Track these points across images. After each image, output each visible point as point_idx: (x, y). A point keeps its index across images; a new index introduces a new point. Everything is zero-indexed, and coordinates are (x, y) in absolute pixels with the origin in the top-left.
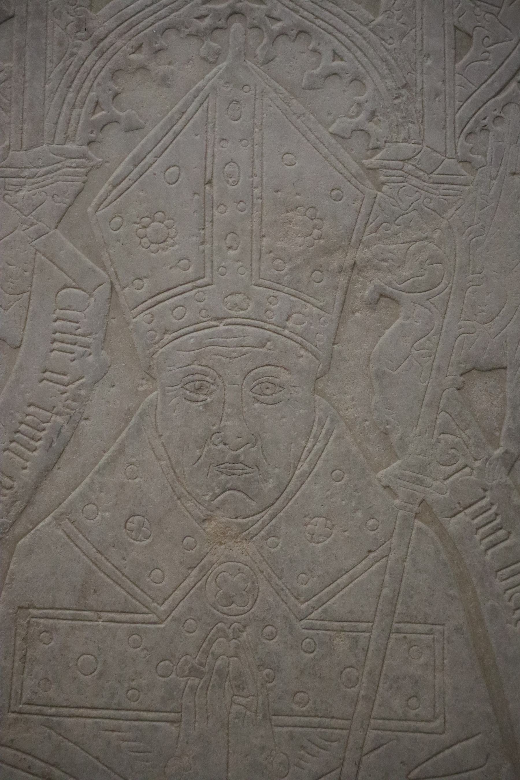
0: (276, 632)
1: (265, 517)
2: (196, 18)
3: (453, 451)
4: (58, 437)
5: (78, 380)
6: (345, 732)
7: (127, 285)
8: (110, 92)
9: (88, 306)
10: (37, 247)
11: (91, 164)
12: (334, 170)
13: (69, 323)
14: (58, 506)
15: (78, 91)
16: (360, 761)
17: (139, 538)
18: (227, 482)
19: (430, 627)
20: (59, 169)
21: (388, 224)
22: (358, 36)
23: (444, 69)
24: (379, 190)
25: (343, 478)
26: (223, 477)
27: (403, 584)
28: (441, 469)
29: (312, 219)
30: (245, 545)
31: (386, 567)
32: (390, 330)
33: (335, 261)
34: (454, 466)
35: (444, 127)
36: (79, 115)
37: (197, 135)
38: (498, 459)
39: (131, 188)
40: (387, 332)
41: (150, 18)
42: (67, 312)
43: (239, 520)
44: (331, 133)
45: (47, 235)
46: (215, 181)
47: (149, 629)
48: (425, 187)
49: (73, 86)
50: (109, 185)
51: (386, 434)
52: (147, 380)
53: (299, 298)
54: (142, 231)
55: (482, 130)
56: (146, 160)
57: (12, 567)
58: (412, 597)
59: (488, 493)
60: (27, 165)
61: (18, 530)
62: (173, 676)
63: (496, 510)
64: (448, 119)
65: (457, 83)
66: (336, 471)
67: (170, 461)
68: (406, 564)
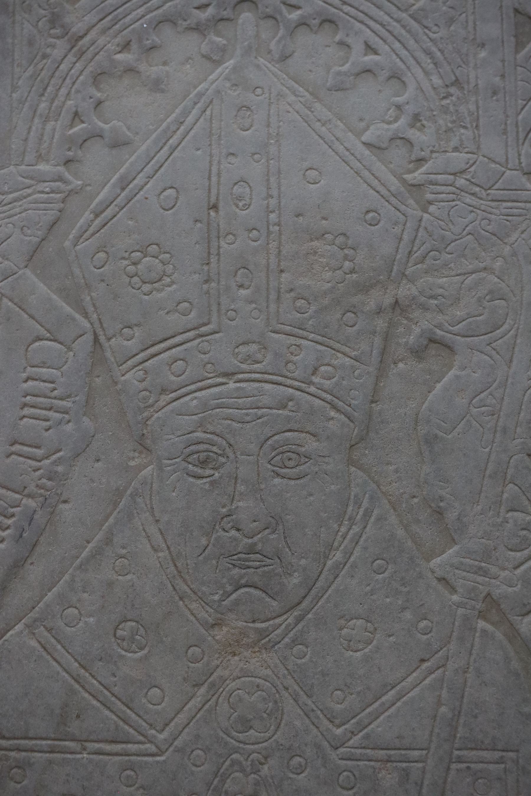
0: (306, 764)
1: (289, 621)
2: (196, 8)
3: (525, 532)
4: (30, 524)
5: (54, 454)
7: (114, 336)
8: (92, 100)
9: (66, 362)
11: (69, 187)
12: (369, 188)
13: (42, 384)
14: (31, 611)
15: (53, 101)
17: (132, 649)
18: (242, 577)
19: (501, 754)
20: (29, 195)
21: (437, 253)
22: (395, 24)
23: (503, 61)
24: (425, 210)
25: (386, 569)
26: (236, 571)
27: (465, 700)
28: (509, 555)
29: (342, 249)
30: (265, 655)
31: (443, 679)
32: (442, 383)
36: (54, 129)
37: (198, 149)
39: (118, 216)
40: (439, 386)
41: (139, 11)
44: (364, 143)
45: (15, 276)
46: (221, 205)
47: (146, 763)
48: (482, 206)
49: (46, 95)
50: (91, 213)
51: (439, 513)
52: (141, 453)
53: (328, 347)
54: (131, 269)
56: (135, 182)
58: (476, 717)
64: (508, 122)
65: (519, 77)
66: (378, 561)
67: (170, 552)
68: (468, 675)
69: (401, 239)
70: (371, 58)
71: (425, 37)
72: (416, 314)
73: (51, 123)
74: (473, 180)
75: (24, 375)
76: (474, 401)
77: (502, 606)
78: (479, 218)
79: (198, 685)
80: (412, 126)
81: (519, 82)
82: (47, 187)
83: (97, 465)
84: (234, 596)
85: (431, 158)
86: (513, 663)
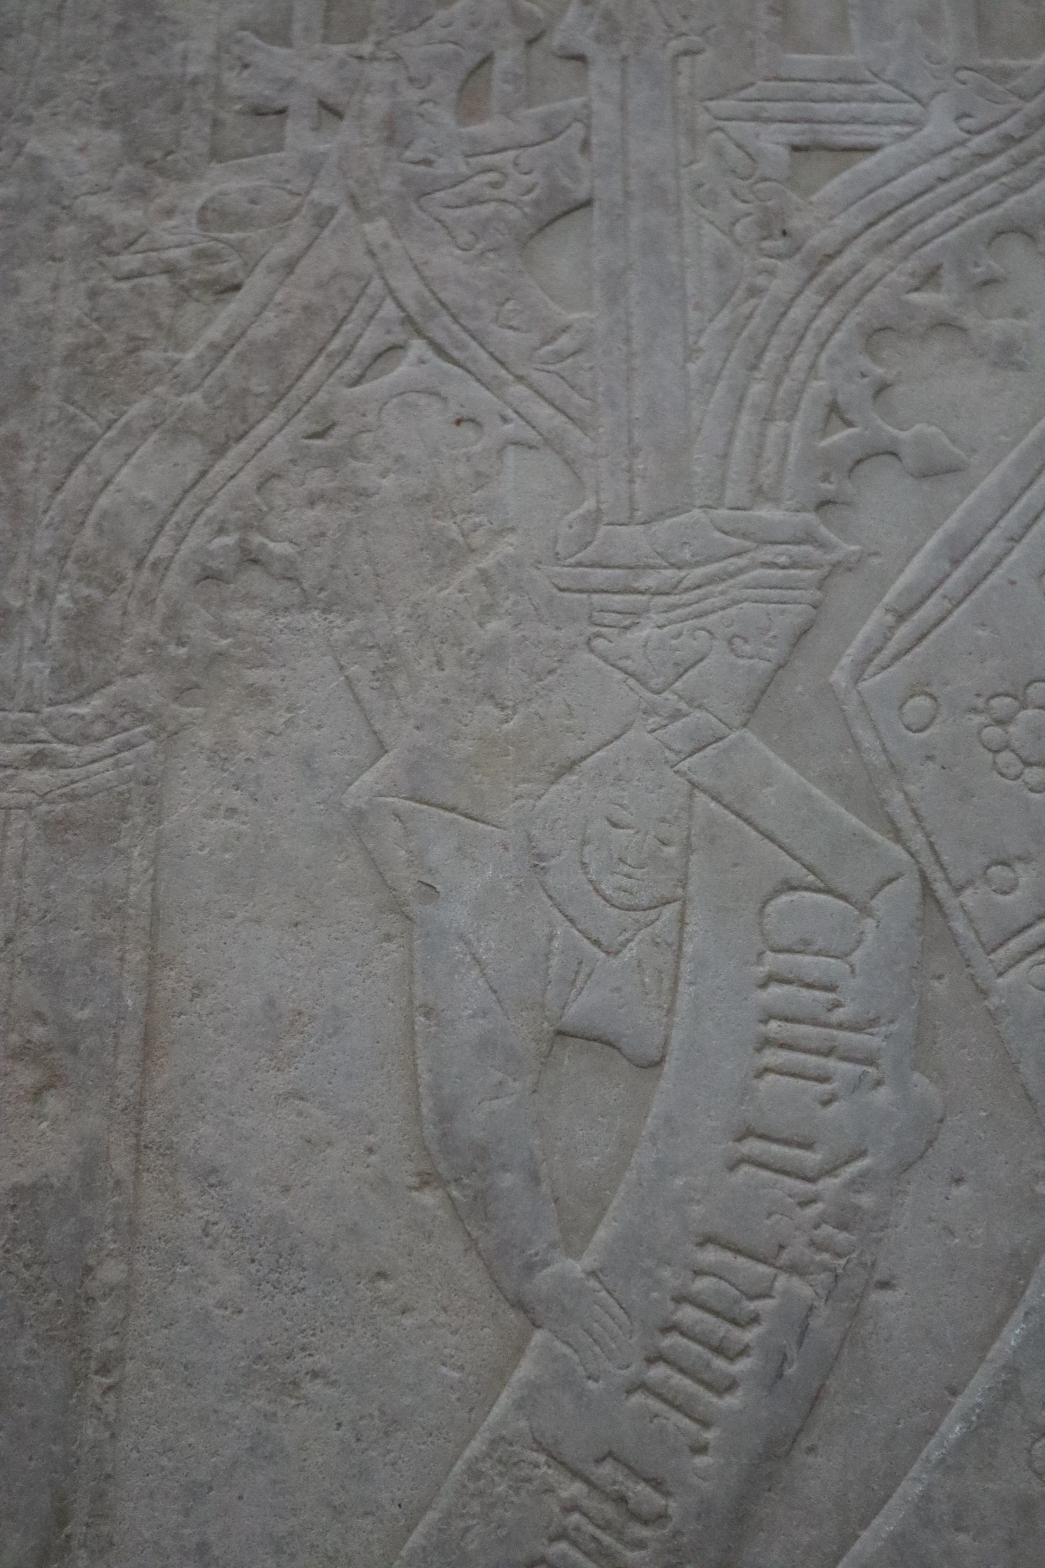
4: (800, 1343)
5: (847, 1163)
7: (970, 883)
8: (866, 380)
9: (859, 942)
10: (695, 778)
11: (834, 557)
13: (805, 992)
15: (778, 381)
20: (741, 571)
36: (787, 437)
39: (951, 620)
41: (951, 210)
42: (799, 957)
45: (720, 744)
49: (763, 366)
54: (993, 733)
56: (984, 547)
60: (651, 561)
73: (778, 423)
75: (763, 970)
82: (782, 554)
83: (956, 1191)
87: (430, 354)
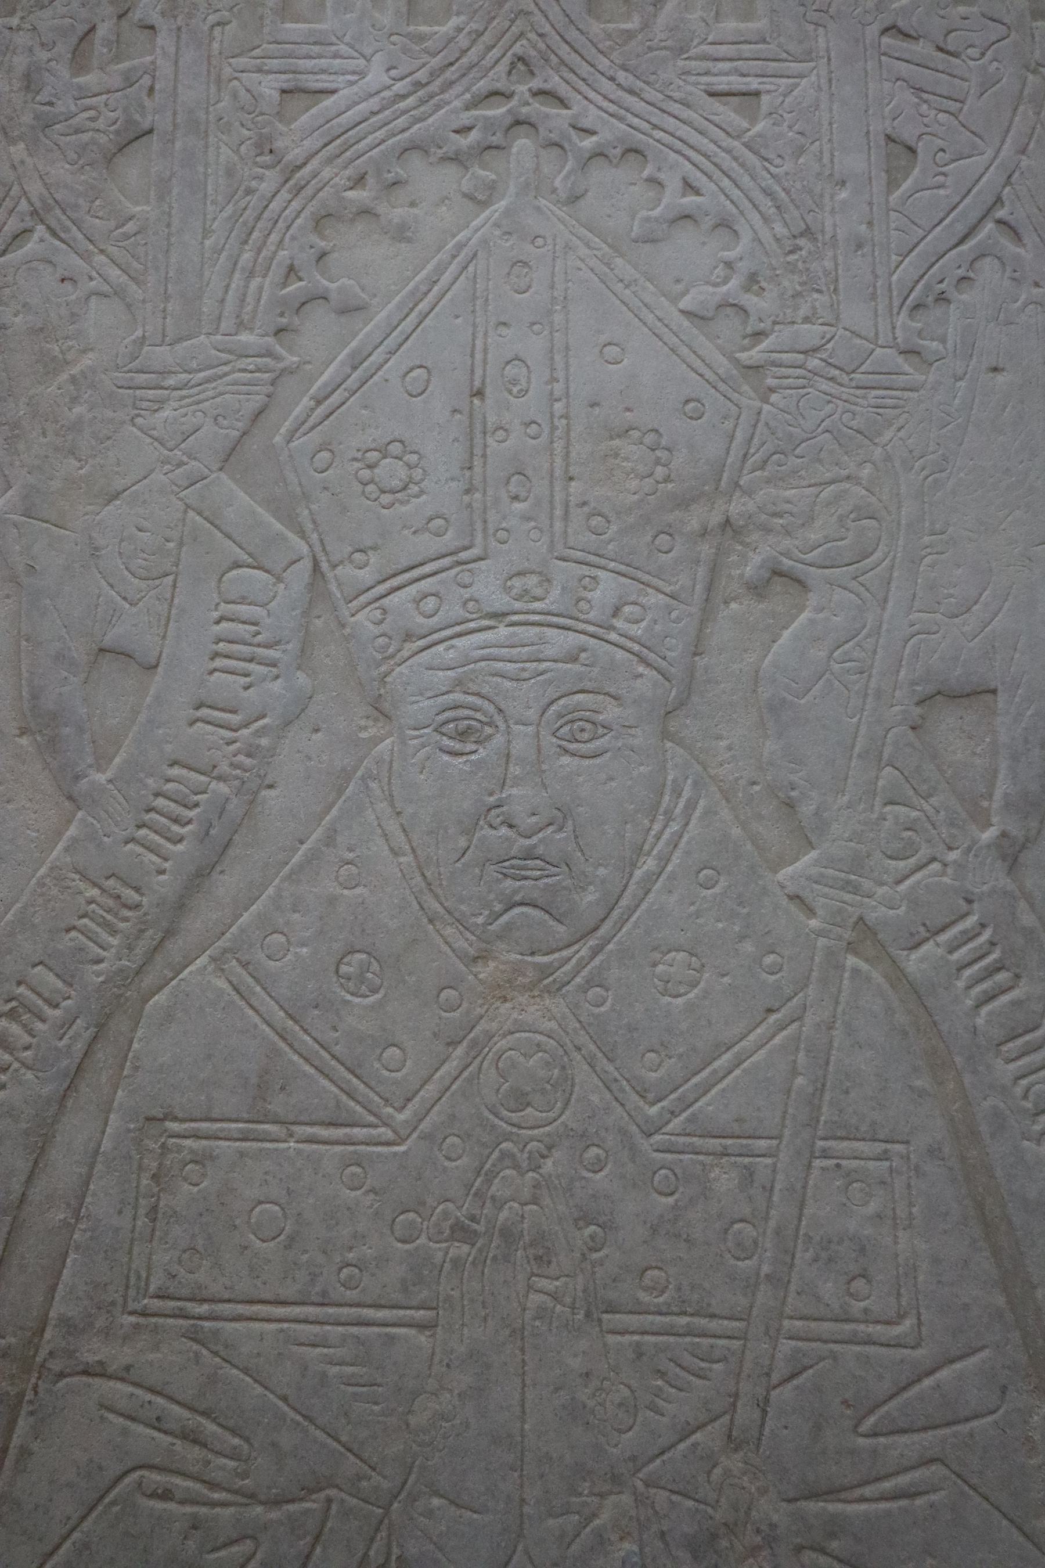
0: (606, 1158)
1: (582, 953)
2: (456, 132)
3: (910, 833)
4: (220, 818)
6: (736, 1344)
7: (341, 562)
8: (313, 250)
9: (274, 597)
10: (188, 501)
11: (281, 365)
13: (240, 626)
14: (219, 938)
15: (259, 251)
16: (767, 1400)
17: (362, 992)
18: (515, 892)
19: (884, 1146)
20: (226, 375)
21: (782, 456)
22: (723, 154)
23: (870, 204)
24: (765, 400)
25: (717, 882)
26: (509, 882)
27: (831, 1069)
29: (653, 450)
30: (548, 1001)
31: (799, 1038)
32: (790, 630)
33: (693, 520)
34: (912, 861)
35: (874, 297)
36: (261, 289)
37: (457, 317)
38: (989, 846)
39: (348, 403)
40: (786, 634)
41: (377, 134)
42: (239, 606)
43: (538, 959)
44: (682, 311)
46: (488, 391)
47: (379, 1155)
49: (250, 242)
50: (311, 399)
51: (790, 805)
52: (376, 720)
53: (633, 579)
54: (365, 474)
55: (937, 300)
56: (372, 358)
57: (135, 1045)
58: (847, 1092)
59: (976, 906)
60: (173, 369)
61: (148, 981)
62: (423, 1240)
63: (992, 936)
64: (879, 284)
65: (893, 225)
66: (705, 872)
67: (416, 857)
68: (835, 1033)
69: (732, 437)
70: (691, 199)
71: (764, 173)
72: (755, 536)
73: (257, 279)
74: (830, 361)
75: (216, 615)
76: (835, 654)
77: (880, 937)
78: (839, 410)
79: (453, 1043)
80: (747, 289)
81: (892, 232)
82: (250, 364)
83: (314, 737)
84: (505, 918)
85: (773, 331)
86: (897, 1016)
87: (47, 236)
